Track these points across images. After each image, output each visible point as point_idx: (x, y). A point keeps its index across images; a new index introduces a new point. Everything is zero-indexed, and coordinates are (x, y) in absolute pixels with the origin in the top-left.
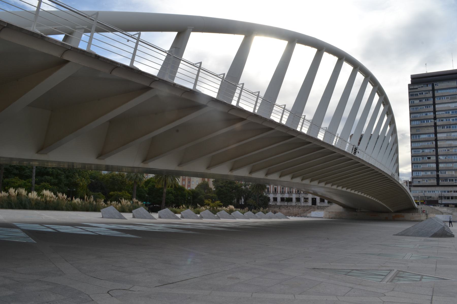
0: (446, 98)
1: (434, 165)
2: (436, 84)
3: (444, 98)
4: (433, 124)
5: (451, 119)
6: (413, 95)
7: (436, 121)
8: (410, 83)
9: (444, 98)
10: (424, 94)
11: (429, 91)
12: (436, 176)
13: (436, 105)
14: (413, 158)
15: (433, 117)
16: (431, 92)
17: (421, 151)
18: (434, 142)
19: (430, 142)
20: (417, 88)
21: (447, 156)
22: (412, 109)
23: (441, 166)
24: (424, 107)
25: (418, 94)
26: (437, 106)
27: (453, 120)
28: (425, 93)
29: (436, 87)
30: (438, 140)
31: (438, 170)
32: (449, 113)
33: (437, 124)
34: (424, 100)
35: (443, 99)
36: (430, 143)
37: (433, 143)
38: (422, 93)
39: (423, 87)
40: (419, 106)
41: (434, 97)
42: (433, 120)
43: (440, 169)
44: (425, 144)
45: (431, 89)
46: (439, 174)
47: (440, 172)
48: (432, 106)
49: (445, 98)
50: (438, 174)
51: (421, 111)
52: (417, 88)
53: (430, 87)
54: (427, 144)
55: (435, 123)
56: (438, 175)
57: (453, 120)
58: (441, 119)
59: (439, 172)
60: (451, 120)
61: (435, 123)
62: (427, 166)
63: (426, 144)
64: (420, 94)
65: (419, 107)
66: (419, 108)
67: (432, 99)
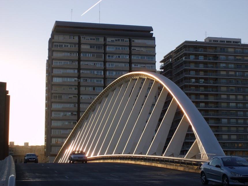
2: (82, 37)
3: (89, 54)
4: (77, 84)
6: (57, 46)
7: (79, 80)
10: (69, 46)
11: (75, 44)
14: (52, 121)
15: (77, 75)
16: (77, 46)
17: (62, 114)
18: (77, 105)
19: (72, 104)
24: (69, 62)
25: (63, 46)
26: (81, 63)
27: (97, 81)
28: (70, 46)
29: (83, 40)
30: (81, 103)
32: (94, 72)
33: (81, 84)
35: (88, 55)
36: (72, 105)
38: (67, 46)
40: (63, 61)
41: (79, 52)
42: (77, 79)
44: (68, 106)
45: (77, 42)
48: (77, 62)
49: (90, 56)
51: (65, 67)
54: (69, 106)
55: (79, 83)
57: (97, 81)
61: (79, 83)
63: (68, 106)
64: (65, 46)
65: (63, 62)
66: (63, 63)
67: (77, 54)
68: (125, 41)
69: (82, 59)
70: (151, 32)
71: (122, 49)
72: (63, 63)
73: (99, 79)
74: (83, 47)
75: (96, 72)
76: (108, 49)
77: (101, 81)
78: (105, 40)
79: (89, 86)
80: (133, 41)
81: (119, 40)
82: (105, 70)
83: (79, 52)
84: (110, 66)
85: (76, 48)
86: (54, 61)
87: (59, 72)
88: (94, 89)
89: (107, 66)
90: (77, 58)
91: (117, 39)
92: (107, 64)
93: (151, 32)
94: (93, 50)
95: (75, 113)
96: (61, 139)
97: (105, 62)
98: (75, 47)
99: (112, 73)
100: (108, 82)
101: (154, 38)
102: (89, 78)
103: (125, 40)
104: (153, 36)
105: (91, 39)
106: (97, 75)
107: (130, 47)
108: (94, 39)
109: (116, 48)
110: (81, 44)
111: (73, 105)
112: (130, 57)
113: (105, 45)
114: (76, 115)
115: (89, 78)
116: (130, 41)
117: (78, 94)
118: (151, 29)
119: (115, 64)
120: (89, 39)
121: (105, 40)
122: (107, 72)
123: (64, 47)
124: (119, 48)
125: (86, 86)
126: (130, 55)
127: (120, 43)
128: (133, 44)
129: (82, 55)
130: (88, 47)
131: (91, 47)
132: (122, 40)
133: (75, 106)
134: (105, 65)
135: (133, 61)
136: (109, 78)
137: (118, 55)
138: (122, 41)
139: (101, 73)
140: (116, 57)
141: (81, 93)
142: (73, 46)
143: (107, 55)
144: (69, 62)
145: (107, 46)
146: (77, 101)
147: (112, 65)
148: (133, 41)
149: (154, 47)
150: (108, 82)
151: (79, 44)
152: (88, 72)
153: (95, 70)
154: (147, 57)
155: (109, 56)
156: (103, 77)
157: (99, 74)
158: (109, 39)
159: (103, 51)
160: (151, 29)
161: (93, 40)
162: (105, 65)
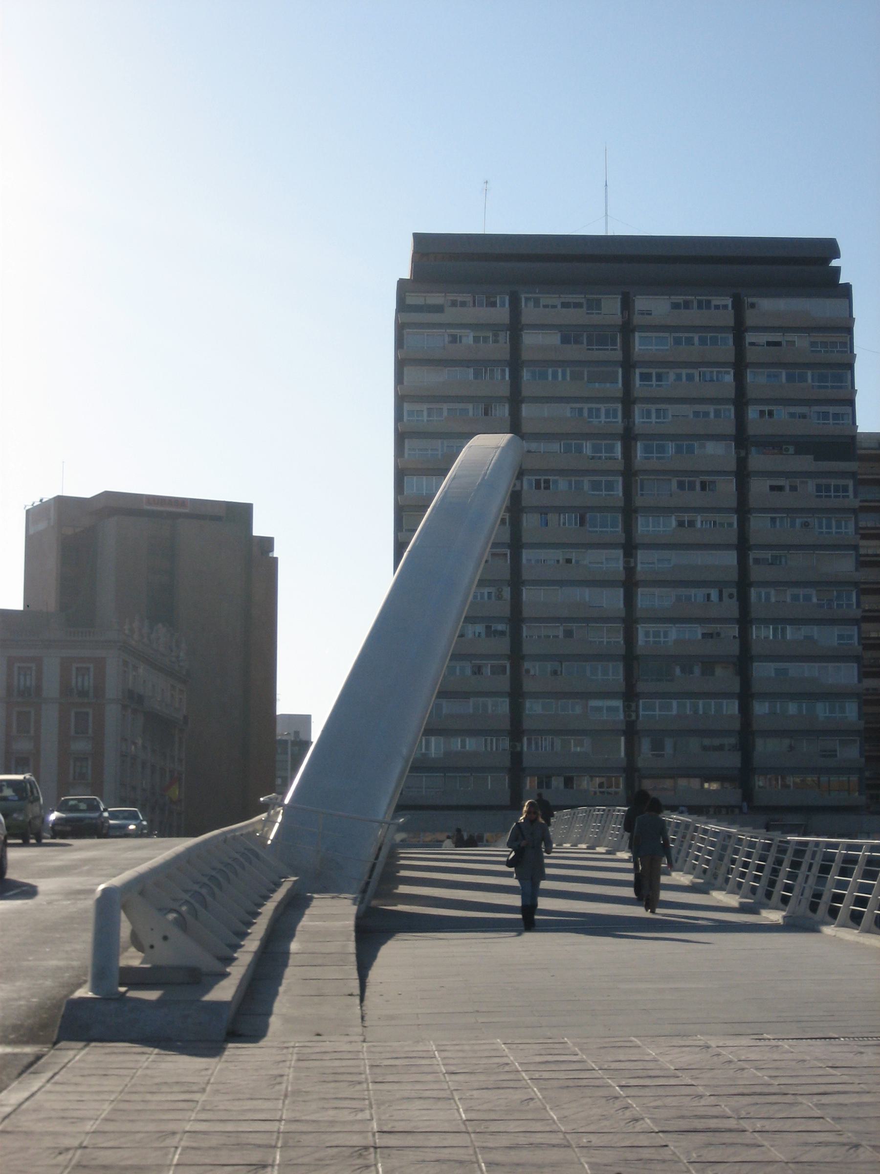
0: (568, 378)
1: (503, 706)
2: (527, 299)
3: (560, 370)
5: (586, 482)
8: (407, 275)
9: (560, 370)
11: (495, 328)
12: (507, 762)
13: (522, 402)
16: (504, 337)
18: (507, 592)
20: (439, 309)
21: (561, 662)
22: (411, 413)
23: (533, 708)
27: (596, 486)
29: (529, 313)
30: (523, 583)
31: (516, 731)
32: (579, 449)
34: (471, 370)
36: (489, 593)
37: (499, 597)
39: (463, 304)
41: (515, 363)
43: (527, 724)
46: (522, 747)
47: (525, 739)
49: (564, 374)
50: (519, 749)
52: (439, 309)
53: (501, 314)
56: (516, 757)
57: (596, 486)
58: (543, 478)
59: (520, 740)
60: (586, 486)
62: (471, 711)
65: (445, 407)
66: (445, 413)
67: (507, 370)
68: (717, 307)
69: (526, 392)
70: (834, 263)
71: (703, 341)
72: (445, 413)
73: (603, 479)
74: (529, 339)
75: (587, 448)
76: (640, 346)
77: (610, 486)
78: (627, 305)
79: (559, 510)
80: (753, 306)
81: (687, 305)
82: (628, 437)
83: (515, 363)
84: (649, 416)
85: (501, 348)
86: (406, 405)
87: (430, 452)
88: (582, 522)
89: (638, 419)
90: (504, 390)
91: (679, 299)
92: (637, 409)
93: (834, 263)
94: (573, 352)
95: (500, 627)
96: (442, 739)
97: (628, 401)
98: (496, 341)
99: (662, 449)
100: (642, 490)
101: (848, 287)
102: (562, 472)
103: (716, 301)
104: (842, 281)
105: (565, 305)
106: (593, 458)
107: (739, 329)
108: (578, 305)
109: (677, 341)
110: (521, 330)
111: (492, 590)
112: (739, 378)
113: (627, 329)
114: (502, 633)
115: (562, 472)
116: (738, 306)
117: (510, 546)
118: (829, 248)
119: (672, 409)
120: (554, 307)
121: (627, 305)
122: (639, 444)
123: (451, 342)
124: (689, 341)
125: (544, 511)
126: (740, 366)
127: (693, 316)
128: (751, 318)
129: (526, 375)
130: (555, 339)
131: (565, 340)
132: (700, 303)
133: (499, 597)
134: (628, 414)
135: (751, 393)
136: (645, 472)
137: (684, 372)
138: (700, 306)
139: (610, 449)
140: (679, 377)
141: (526, 538)
142: (486, 339)
143: (638, 371)
144: (470, 406)
145: (637, 334)
146: (508, 576)
147: (658, 417)
148: (753, 306)
149: (846, 328)
150: (642, 490)
151: (515, 328)
152: (555, 447)
153: (588, 436)
154: (812, 375)
155: (645, 377)
156: (620, 467)
157: (604, 455)
158: (641, 303)
159: (618, 355)
160: (829, 248)
161: (572, 310)
162: (628, 414)
